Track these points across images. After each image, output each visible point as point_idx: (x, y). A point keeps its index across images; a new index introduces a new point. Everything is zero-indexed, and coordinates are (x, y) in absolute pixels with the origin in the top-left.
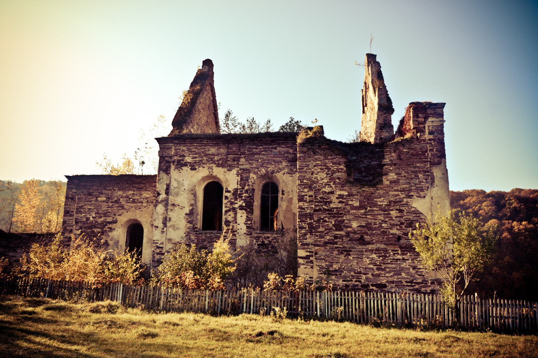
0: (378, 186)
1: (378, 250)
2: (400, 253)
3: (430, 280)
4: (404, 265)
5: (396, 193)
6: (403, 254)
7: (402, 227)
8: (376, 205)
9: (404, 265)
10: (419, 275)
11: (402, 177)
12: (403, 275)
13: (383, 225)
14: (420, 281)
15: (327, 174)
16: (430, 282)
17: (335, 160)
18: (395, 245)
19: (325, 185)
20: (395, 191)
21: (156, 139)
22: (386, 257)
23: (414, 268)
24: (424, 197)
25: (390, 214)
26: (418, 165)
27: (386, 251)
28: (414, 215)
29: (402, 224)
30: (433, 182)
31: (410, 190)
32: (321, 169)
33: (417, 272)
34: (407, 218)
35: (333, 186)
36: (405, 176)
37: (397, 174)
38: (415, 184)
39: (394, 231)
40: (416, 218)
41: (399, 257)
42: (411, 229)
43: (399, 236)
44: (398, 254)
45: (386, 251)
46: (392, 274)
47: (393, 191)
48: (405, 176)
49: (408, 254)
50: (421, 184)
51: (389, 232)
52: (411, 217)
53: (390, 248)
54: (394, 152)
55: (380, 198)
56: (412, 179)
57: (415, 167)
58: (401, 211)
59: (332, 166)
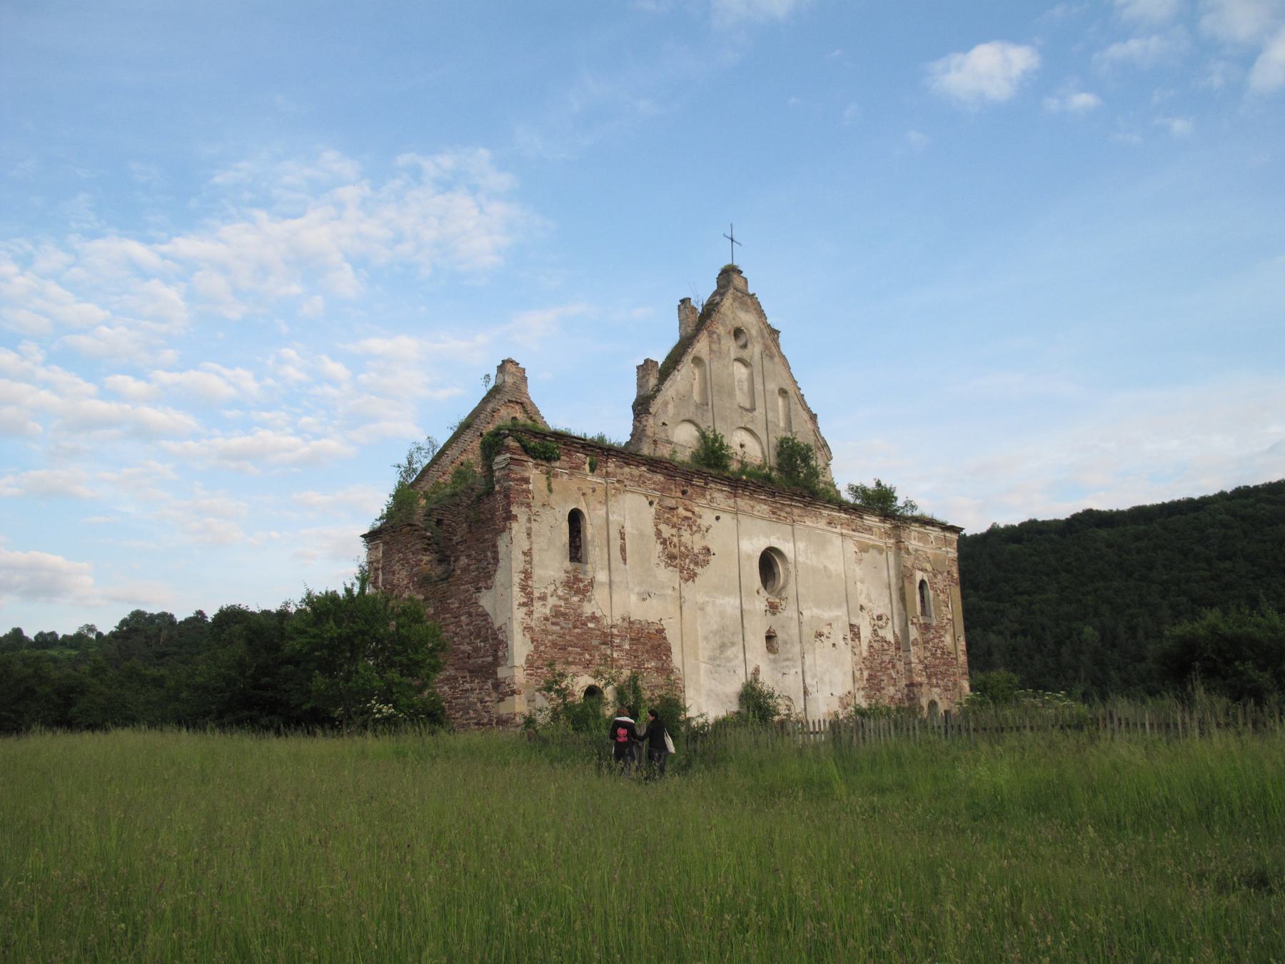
0: (450, 579)
1: (448, 679)
2: (469, 680)
3: (496, 718)
4: (473, 698)
5: (466, 586)
6: (472, 682)
7: (471, 640)
8: (447, 610)
9: (473, 698)
10: (486, 712)
11: (472, 560)
12: (471, 712)
13: (455, 639)
14: (485, 721)
15: (407, 571)
16: (495, 720)
17: (413, 549)
18: (462, 669)
19: (406, 588)
20: (467, 582)
21: (362, 536)
22: (456, 688)
23: (482, 701)
24: (491, 587)
25: (460, 621)
26: (486, 536)
27: (456, 679)
28: (482, 618)
29: (471, 634)
30: (498, 561)
31: (479, 581)
32: (403, 565)
33: (484, 707)
34: (475, 625)
35: (412, 588)
36: (475, 558)
37: (468, 556)
38: (484, 569)
39: (466, 648)
40: (484, 623)
41: (468, 686)
42: (479, 641)
43: (469, 654)
44: (466, 681)
45: (456, 679)
46: (461, 713)
47: (463, 585)
48: (475, 558)
49: (476, 681)
50: (488, 568)
51: (459, 648)
52: (479, 622)
53: (460, 674)
54: (466, 522)
55: (451, 598)
56: (479, 561)
57: (485, 541)
58: (470, 615)
59: (411, 559)
